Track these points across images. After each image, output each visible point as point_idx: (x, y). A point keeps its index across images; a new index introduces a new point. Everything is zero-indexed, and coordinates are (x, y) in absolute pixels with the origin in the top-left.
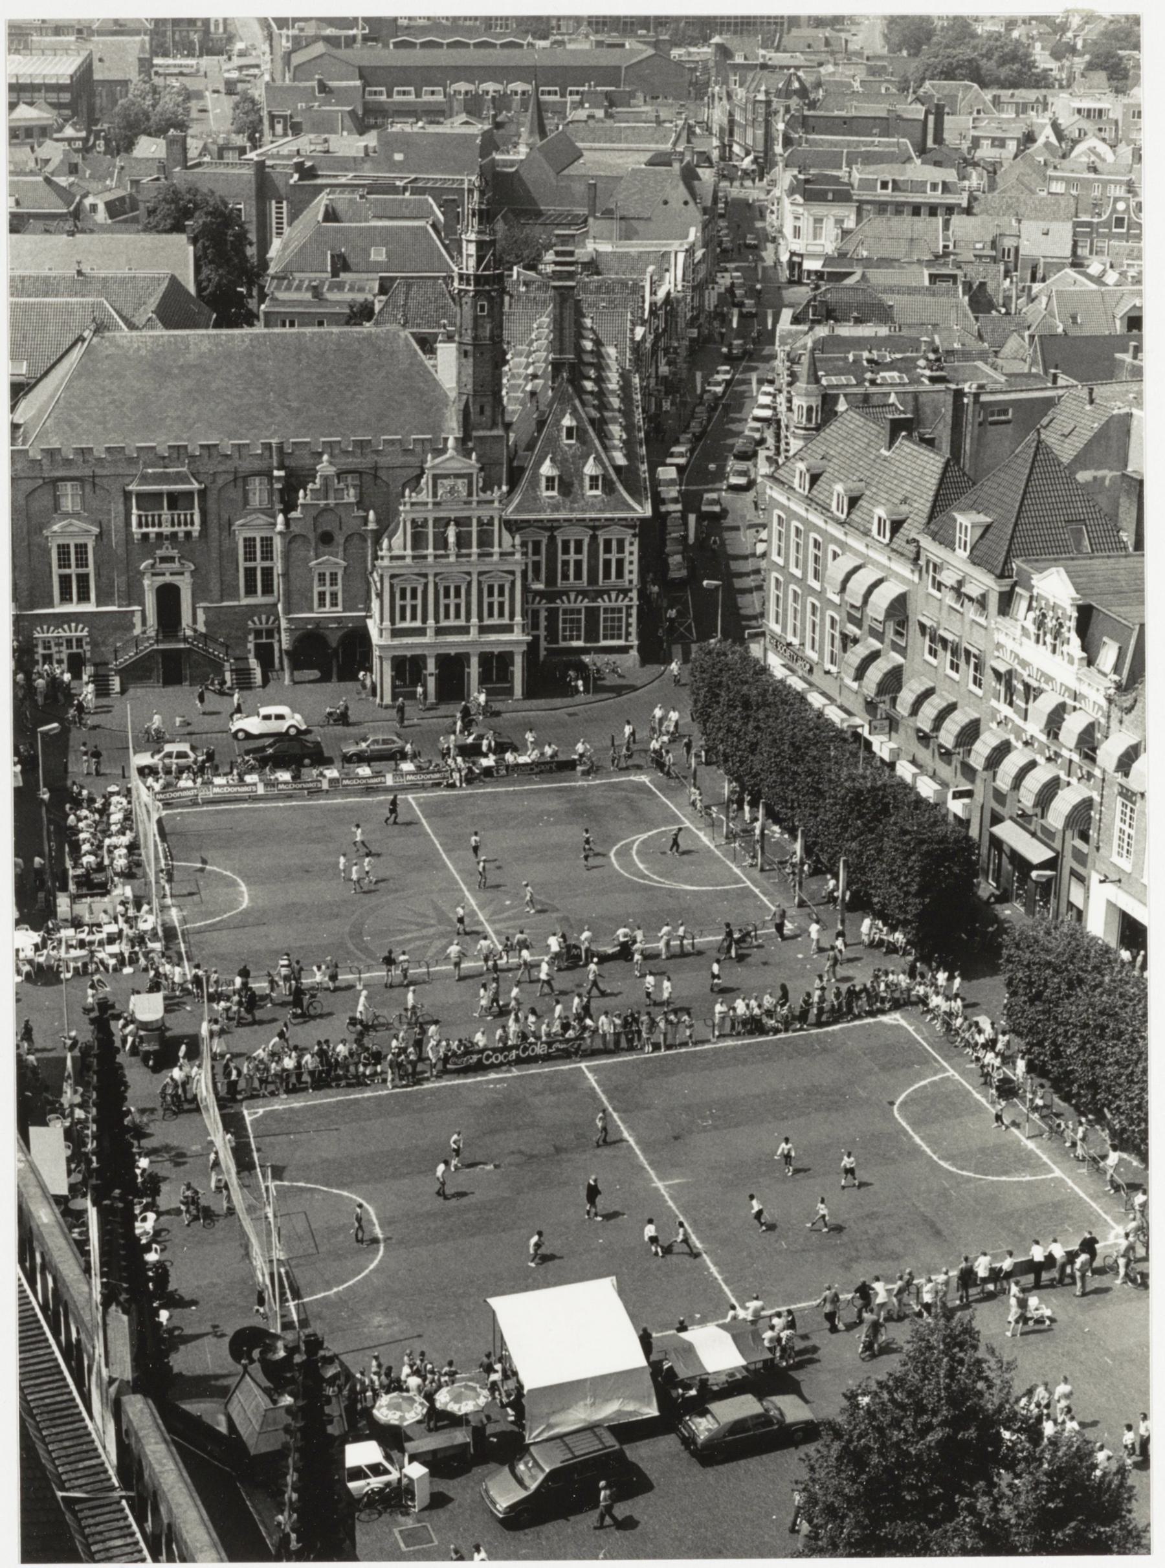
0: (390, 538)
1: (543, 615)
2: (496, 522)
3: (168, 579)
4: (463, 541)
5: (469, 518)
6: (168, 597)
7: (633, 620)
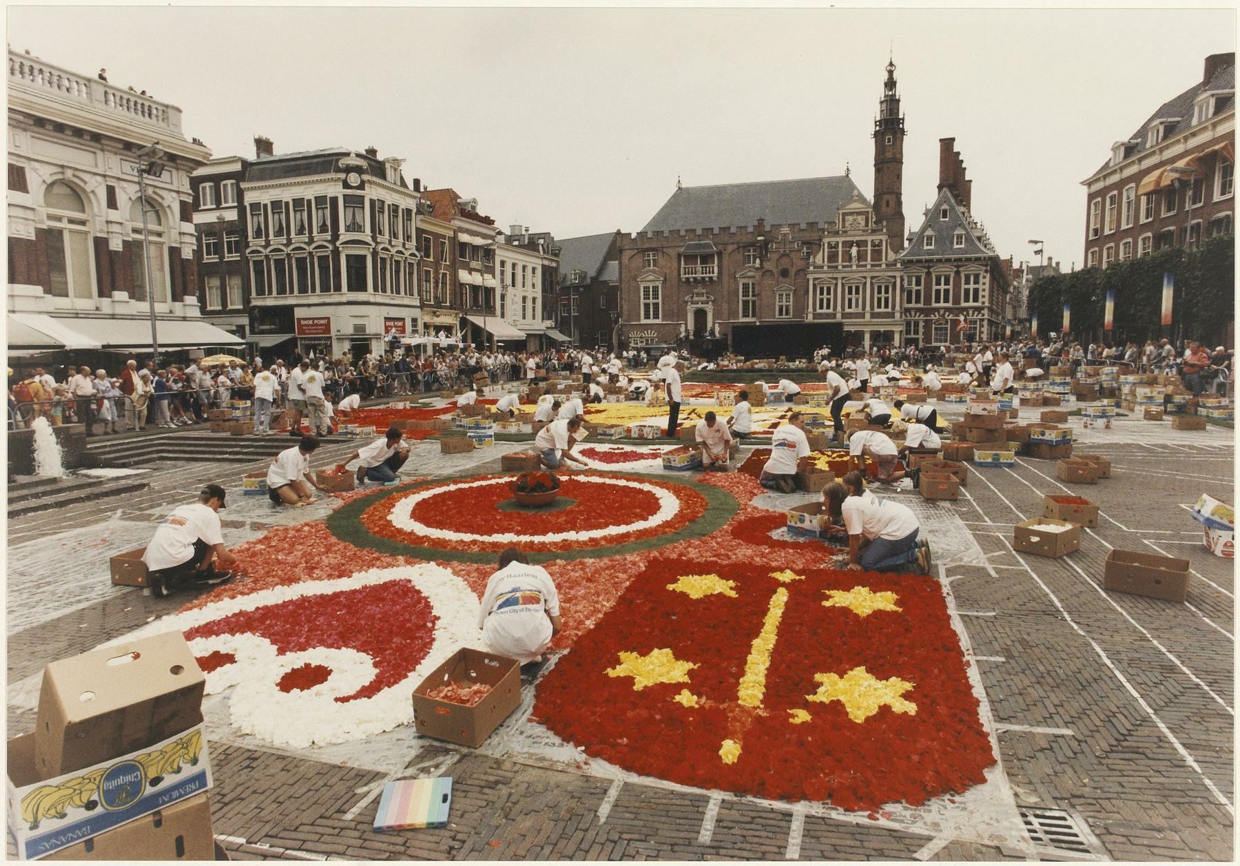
0: (814, 257)
1: (921, 324)
2: (884, 243)
3: (700, 306)
4: (861, 256)
5: (866, 241)
6: (700, 315)
7: (985, 329)
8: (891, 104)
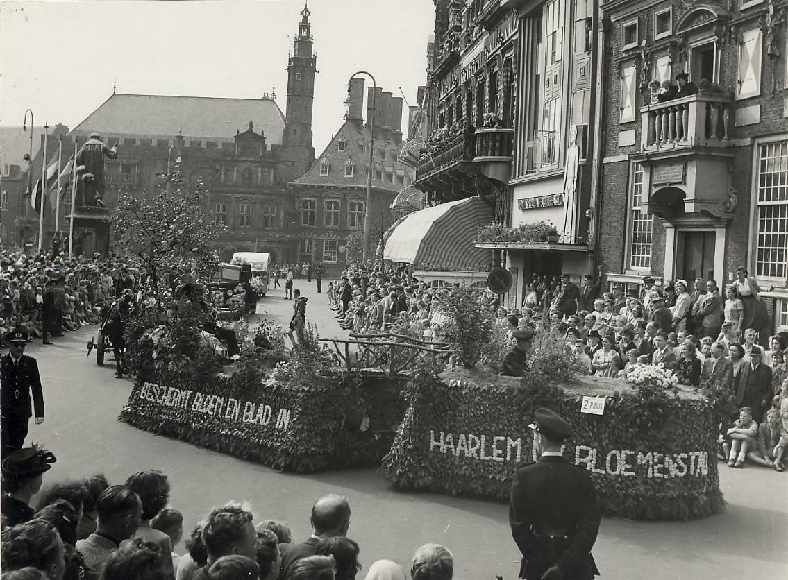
8: (304, 42)
